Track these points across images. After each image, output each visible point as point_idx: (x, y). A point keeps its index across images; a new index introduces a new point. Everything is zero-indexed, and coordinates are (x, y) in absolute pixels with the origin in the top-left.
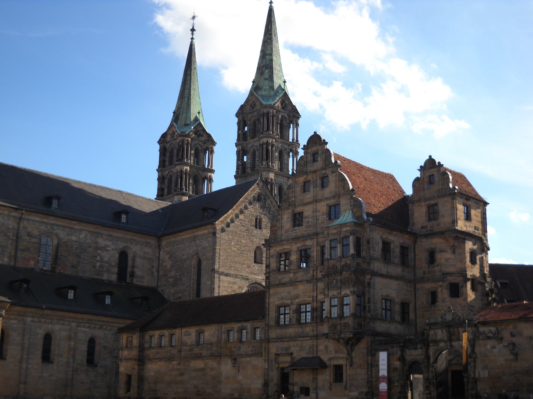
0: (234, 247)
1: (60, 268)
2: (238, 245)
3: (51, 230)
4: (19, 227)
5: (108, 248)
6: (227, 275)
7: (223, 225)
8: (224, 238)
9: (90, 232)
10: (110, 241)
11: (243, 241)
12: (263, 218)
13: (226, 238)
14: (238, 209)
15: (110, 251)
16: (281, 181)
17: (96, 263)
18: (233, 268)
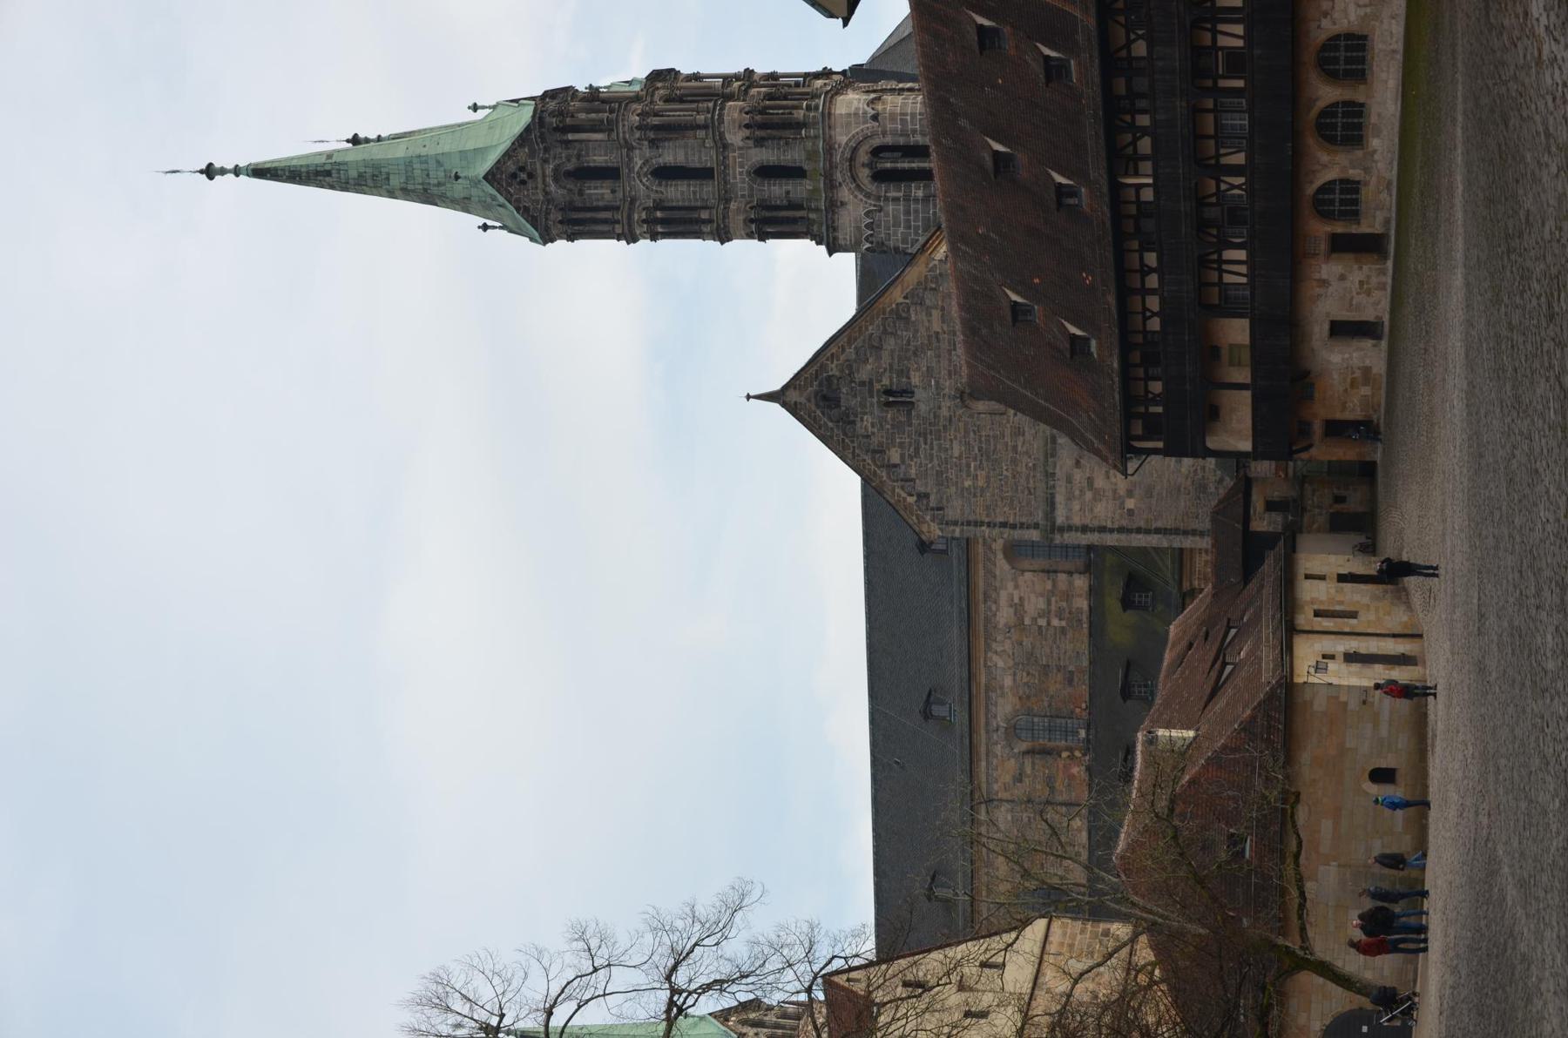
0: (977, 479)
1: (1078, 710)
2: (968, 466)
3: (999, 733)
4: (1007, 801)
5: (1016, 600)
6: (1051, 504)
7: (928, 518)
8: (959, 511)
9: (988, 647)
10: (998, 594)
11: (956, 450)
12: (882, 386)
13: (957, 503)
14: (878, 472)
15: (1022, 595)
16: (741, 173)
17: (1055, 627)
18: (1031, 482)
